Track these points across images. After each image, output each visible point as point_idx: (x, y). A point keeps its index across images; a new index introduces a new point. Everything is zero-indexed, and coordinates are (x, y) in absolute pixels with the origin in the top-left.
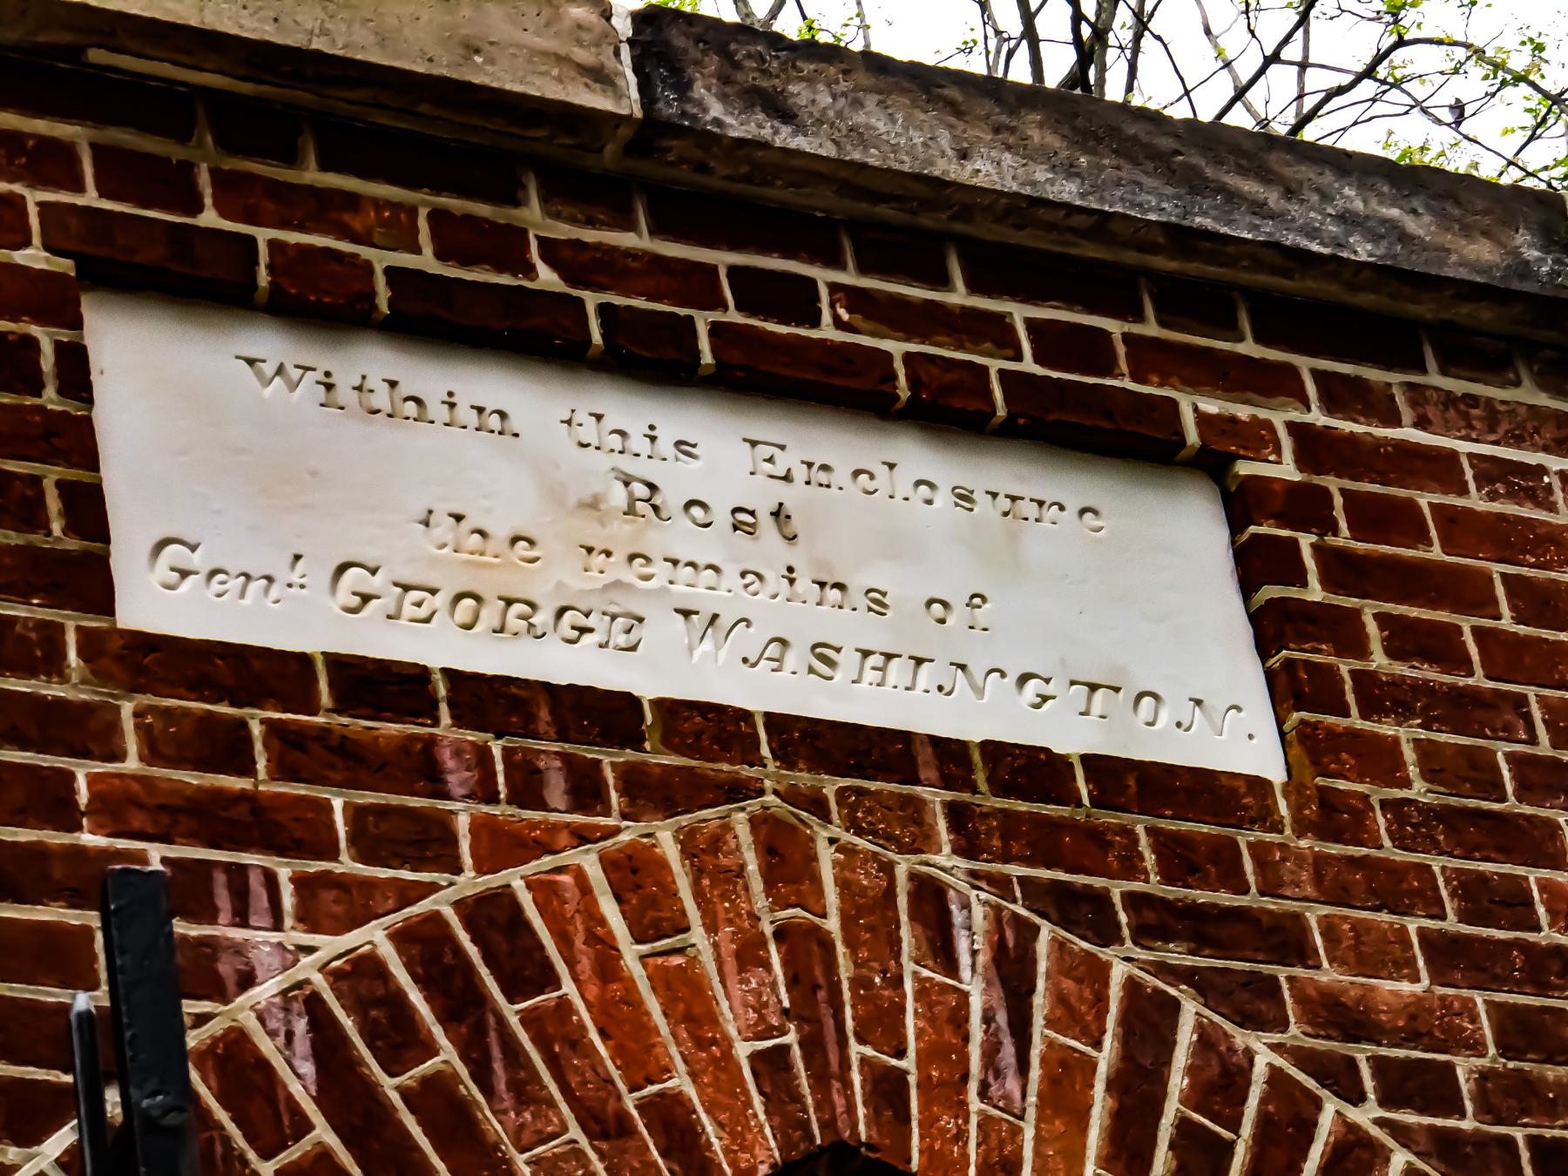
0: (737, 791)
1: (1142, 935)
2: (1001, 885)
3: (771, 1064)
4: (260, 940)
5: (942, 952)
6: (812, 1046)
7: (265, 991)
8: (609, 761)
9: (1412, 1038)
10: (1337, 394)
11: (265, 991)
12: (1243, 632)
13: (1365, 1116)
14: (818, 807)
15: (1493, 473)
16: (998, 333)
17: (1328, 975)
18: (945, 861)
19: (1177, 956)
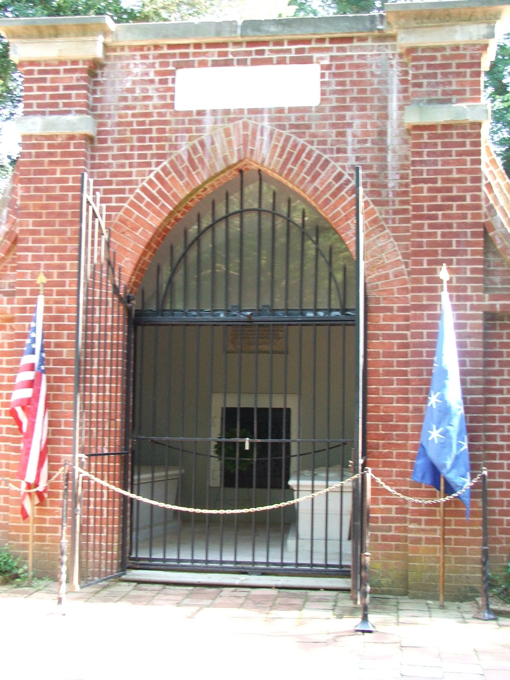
0: (240, 119)
1: (290, 128)
2: (271, 125)
3: (239, 150)
4: (183, 143)
5: (262, 135)
6: (244, 148)
7: (183, 149)
8: (226, 117)
9: (323, 137)
10: (339, 49)
11: (183, 149)
12: (319, 84)
13: (313, 148)
14: (250, 119)
15: (360, 57)
16: (289, 51)
17: (313, 130)
18: (266, 124)
19: (294, 130)
